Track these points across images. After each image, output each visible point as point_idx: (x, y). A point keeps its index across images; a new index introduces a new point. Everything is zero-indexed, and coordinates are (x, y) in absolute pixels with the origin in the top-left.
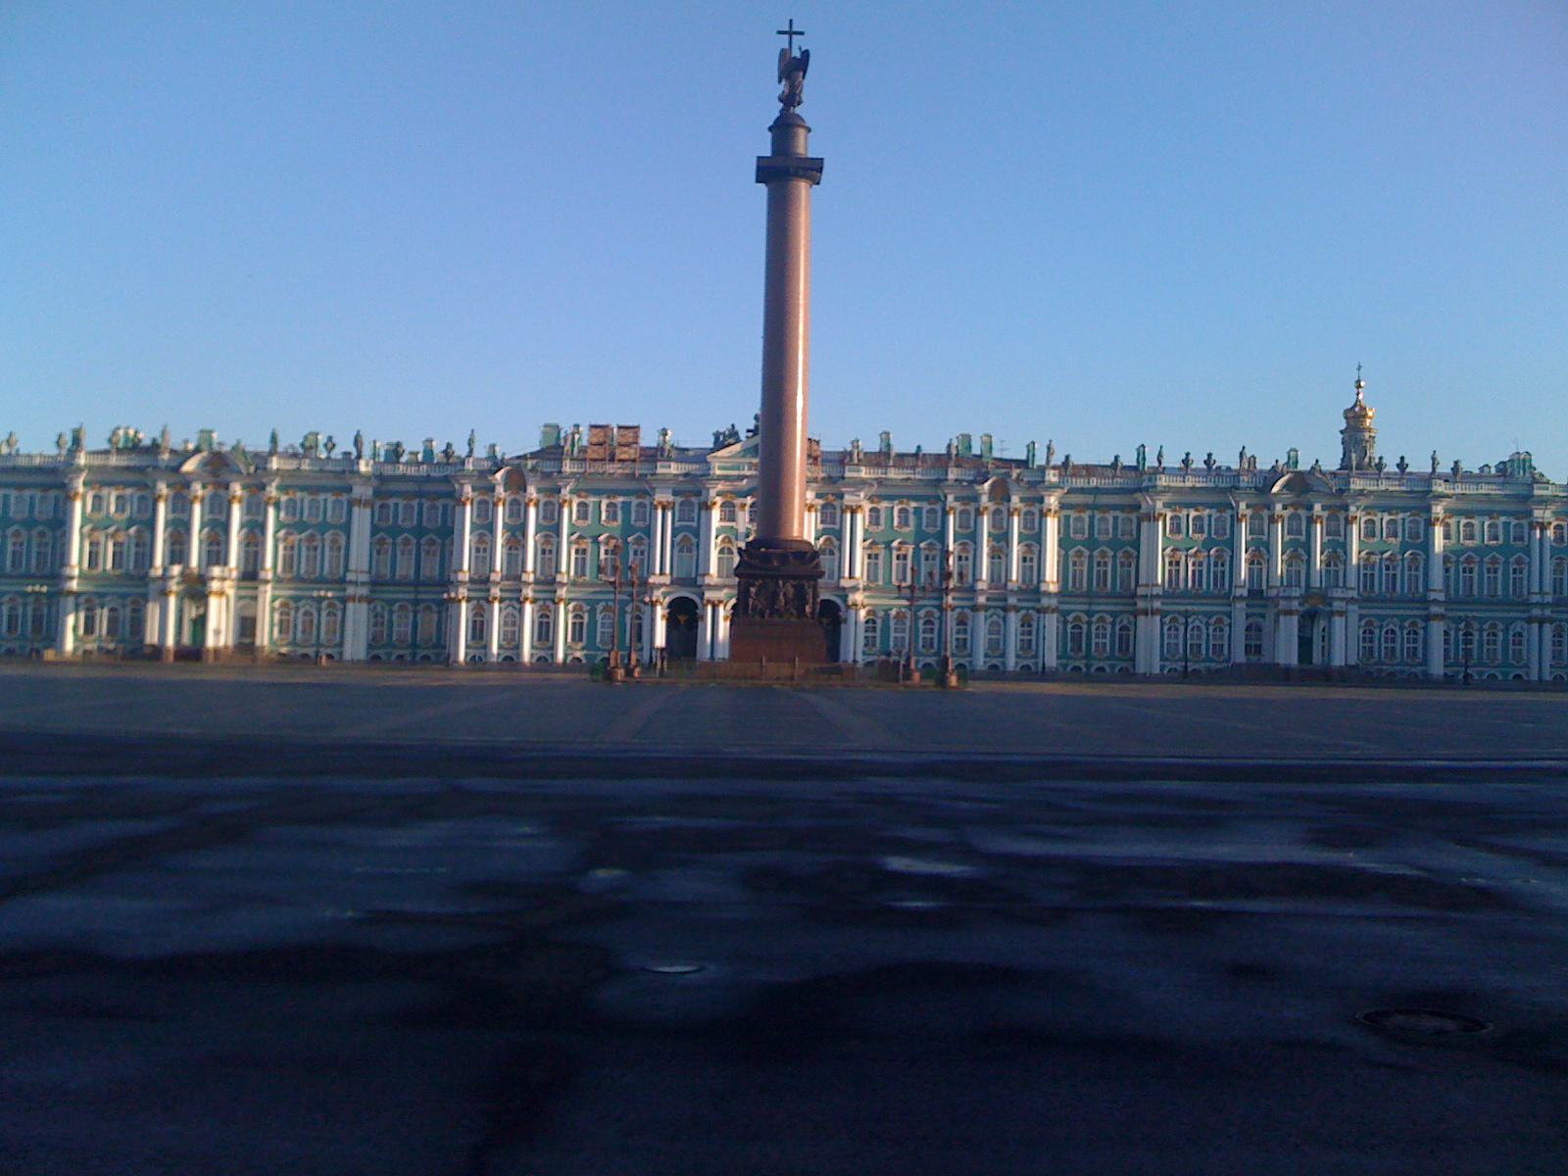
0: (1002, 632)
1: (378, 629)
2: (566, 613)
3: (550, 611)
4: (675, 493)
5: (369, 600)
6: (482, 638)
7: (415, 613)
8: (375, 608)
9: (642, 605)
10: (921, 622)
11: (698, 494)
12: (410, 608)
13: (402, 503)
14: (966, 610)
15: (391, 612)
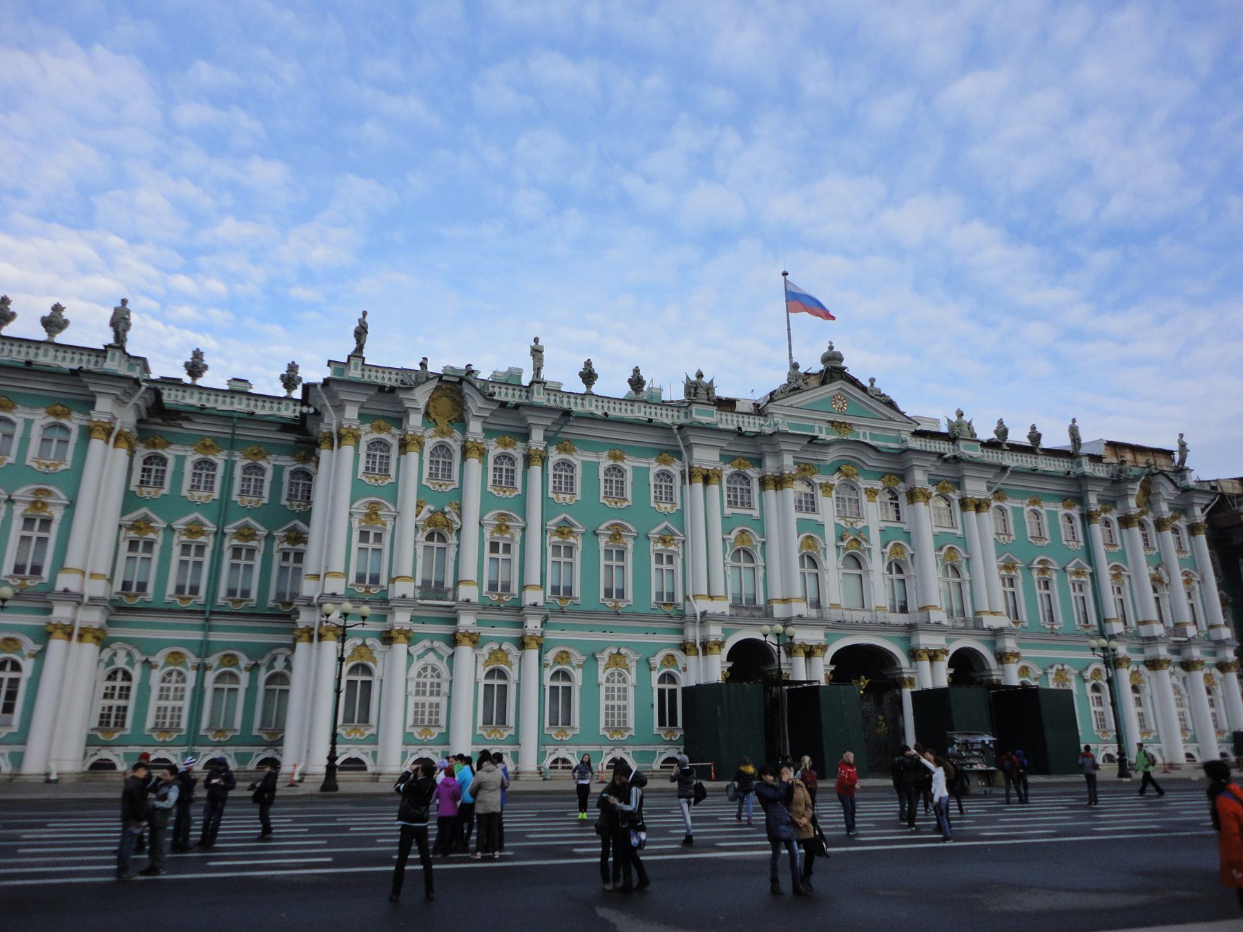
0: (1186, 701)
1: (116, 702)
2: (542, 664)
3: (509, 664)
4: (726, 458)
5: (103, 641)
6: (365, 719)
7: (202, 669)
8: (111, 662)
9: (679, 655)
10: (1089, 686)
11: (758, 462)
12: (192, 660)
13: (192, 457)
14: (1143, 668)
15: (148, 665)
